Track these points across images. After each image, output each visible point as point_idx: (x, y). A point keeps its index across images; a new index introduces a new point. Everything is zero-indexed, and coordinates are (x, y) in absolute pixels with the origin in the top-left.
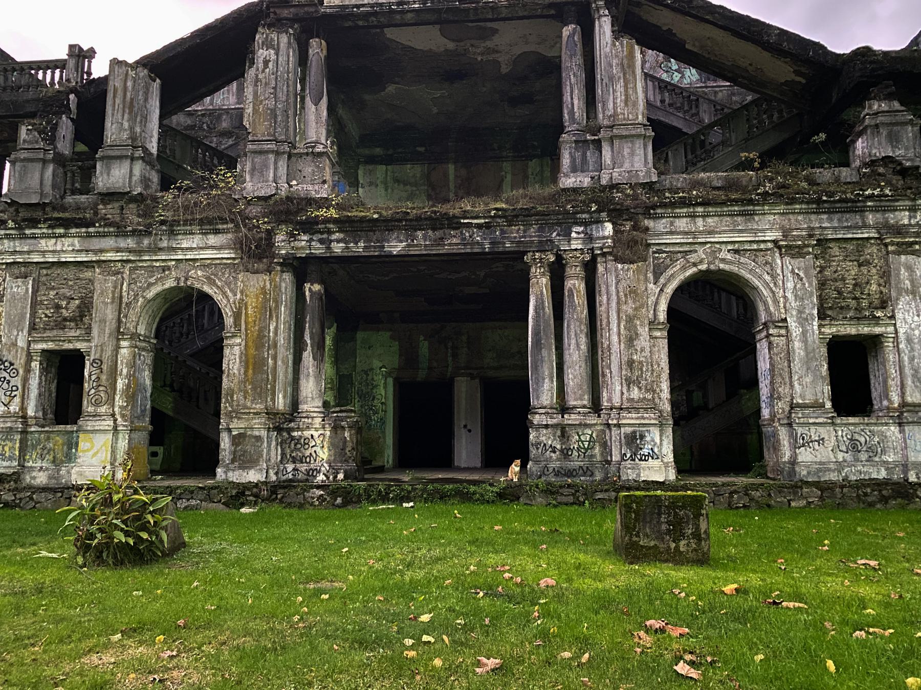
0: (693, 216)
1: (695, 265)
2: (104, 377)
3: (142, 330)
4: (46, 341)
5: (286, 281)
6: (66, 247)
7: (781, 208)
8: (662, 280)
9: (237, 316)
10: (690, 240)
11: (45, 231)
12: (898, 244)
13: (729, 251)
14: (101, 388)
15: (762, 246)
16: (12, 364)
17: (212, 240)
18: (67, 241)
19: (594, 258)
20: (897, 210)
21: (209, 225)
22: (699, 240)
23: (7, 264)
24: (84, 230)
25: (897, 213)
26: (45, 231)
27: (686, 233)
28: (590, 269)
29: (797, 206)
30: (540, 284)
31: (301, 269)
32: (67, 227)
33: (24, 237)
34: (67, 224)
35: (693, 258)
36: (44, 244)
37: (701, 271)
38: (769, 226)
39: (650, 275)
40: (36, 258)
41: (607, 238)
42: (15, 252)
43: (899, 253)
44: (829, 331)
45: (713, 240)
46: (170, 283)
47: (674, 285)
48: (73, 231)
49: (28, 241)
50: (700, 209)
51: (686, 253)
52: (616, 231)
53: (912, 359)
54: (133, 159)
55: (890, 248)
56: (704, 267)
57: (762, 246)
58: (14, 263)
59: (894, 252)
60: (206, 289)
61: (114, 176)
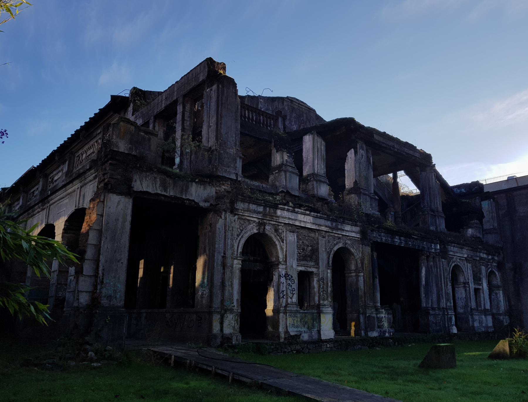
2: (325, 287)
4: (302, 266)
11: (302, 211)
14: (324, 292)
16: (292, 277)
18: (308, 217)
23: (284, 223)
24: (316, 214)
26: (302, 211)
32: (311, 211)
33: (293, 212)
34: (312, 210)
36: (301, 217)
40: (297, 223)
42: (289, 219)
48: (312, 213)
49: (294, 214)
58: (289, 224)
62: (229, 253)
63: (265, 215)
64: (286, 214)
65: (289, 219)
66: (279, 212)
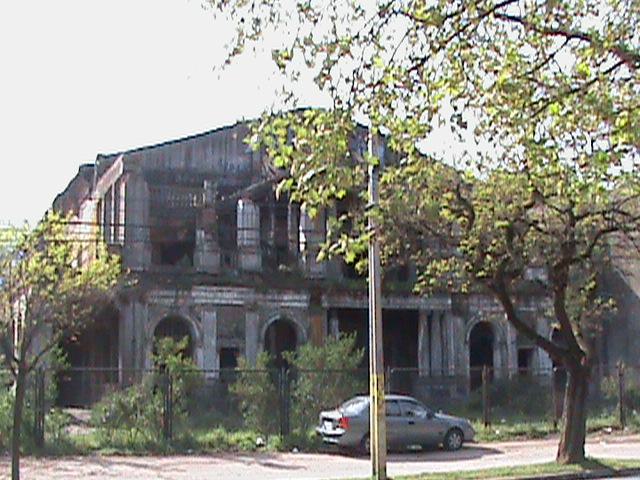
5: (324, 318)
6: (230, 296)
17: (297, 297)
21: (297, 291)
28: (442, 317)
40: (216, 301)
42: (206, 298)
46: (278, 317)
60: (295, 320)
62: (138, 336)
63: (177, 297)
65: (206, 298)
66: (194, 294)
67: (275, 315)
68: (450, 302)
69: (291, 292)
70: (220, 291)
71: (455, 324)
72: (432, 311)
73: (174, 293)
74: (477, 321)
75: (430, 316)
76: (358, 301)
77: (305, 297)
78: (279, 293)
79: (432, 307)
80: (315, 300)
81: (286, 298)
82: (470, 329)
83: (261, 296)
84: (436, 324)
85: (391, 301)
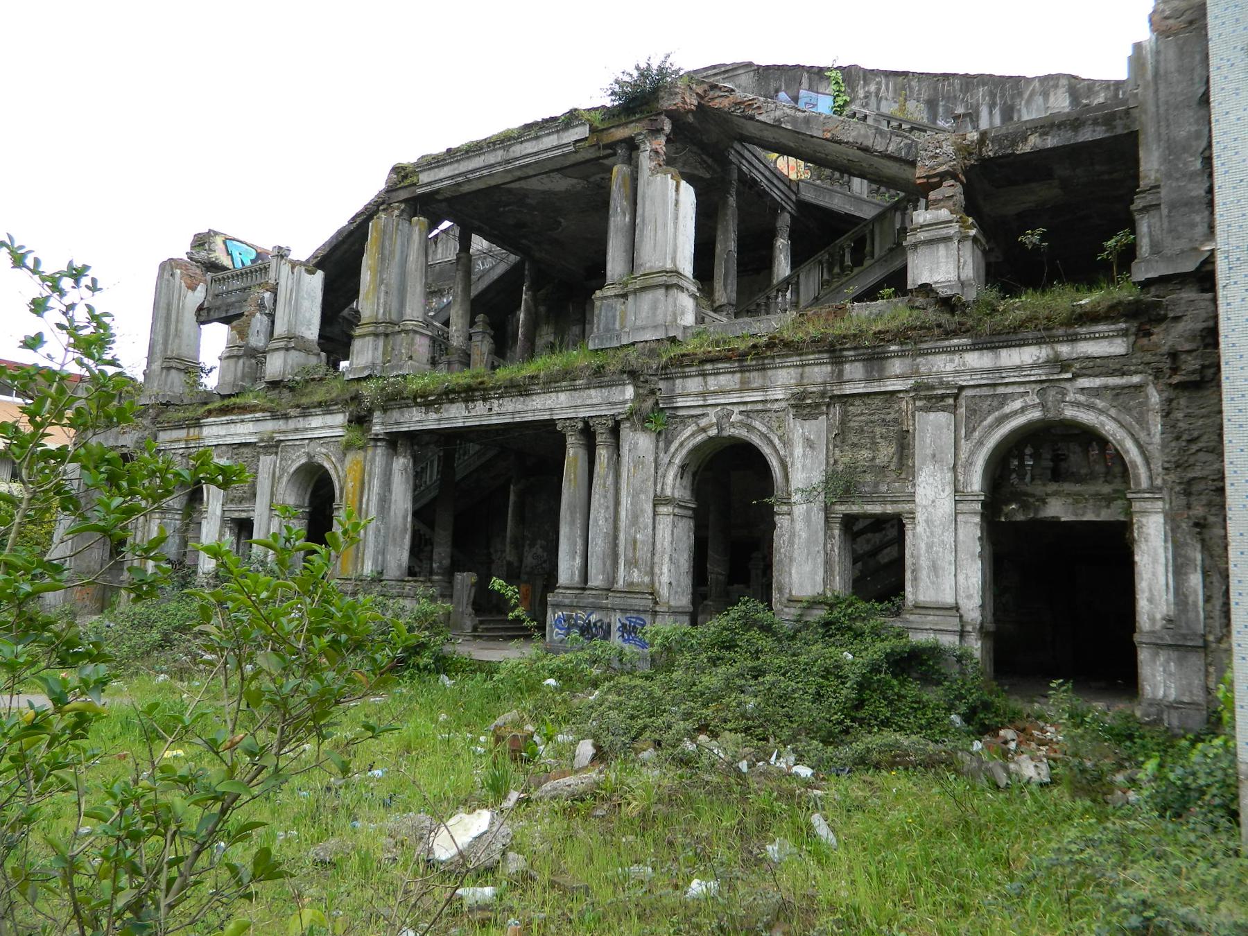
0: (704, 375)
1: (704, 430)
3: (291, 500)
7: (795, 360)
8: (672, 449)
9: (341, 492)
10: (701, 403)
12: (925, 397)
13: (741, 412)
15: (776, 406)
17: (329, 420)
19: (617, 424)
20: (927, 354)
21: (326, 407)
22: (710, 402)
25: (930, 357)
27: (697, 395)
29: (811, 357)
30: (574, 452)
31: (394, 441)
35: (703, 422)
37: (711, 438)
38: (783, 380)
39: (662, 444)
40: (229, 441)
41: (625, 402)
42: (218, 436)
43: (928, 409)
44: (841, 509)
45: (722, 401)
46: (303, 461)
47: (684, 451)
50: (708, 367)
51: (697, 416)
52: (637, 395)
53: (930, 547)
54: (287, 350)
55: (919, 403)
56: (713, 432)
57: (776, 406)
59: (921, 409)
60: (327, 465)
61: (275, 365)
64: (215, 430)
66: (206, 431)
67: (299, 457)
68: (629, 392)
69: (318, 411)
70: (233, 422)
71: (638, 443)
72: (585, 421)
73: (182, 434)
74: (700, 438)
75: (588, 433)
76: (432, 416)
77: (340, 419)
78: (304, 416)
79: (584, 413)
80: (360, 421)
81: (316, 422)
82: (677, 461)
83: (281, 424)
84: (603, 454)
85: (496, 409)
